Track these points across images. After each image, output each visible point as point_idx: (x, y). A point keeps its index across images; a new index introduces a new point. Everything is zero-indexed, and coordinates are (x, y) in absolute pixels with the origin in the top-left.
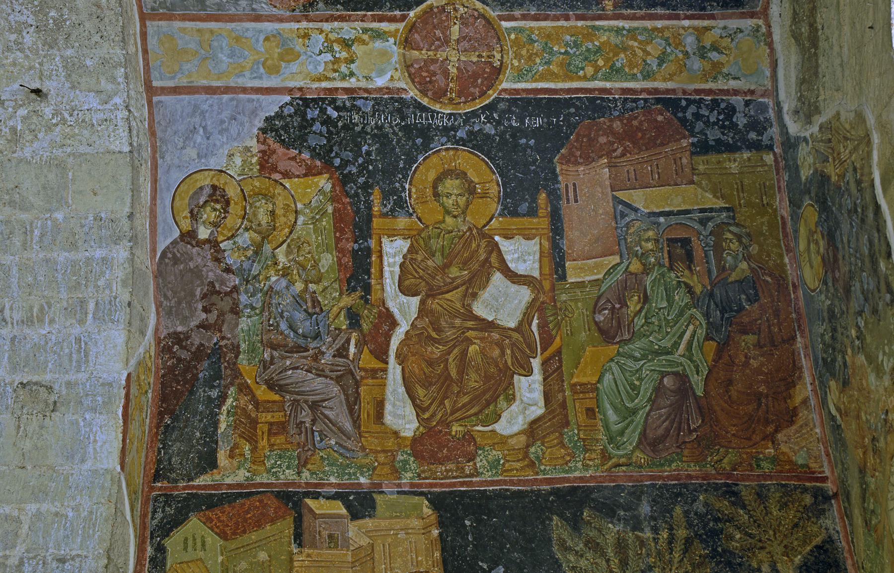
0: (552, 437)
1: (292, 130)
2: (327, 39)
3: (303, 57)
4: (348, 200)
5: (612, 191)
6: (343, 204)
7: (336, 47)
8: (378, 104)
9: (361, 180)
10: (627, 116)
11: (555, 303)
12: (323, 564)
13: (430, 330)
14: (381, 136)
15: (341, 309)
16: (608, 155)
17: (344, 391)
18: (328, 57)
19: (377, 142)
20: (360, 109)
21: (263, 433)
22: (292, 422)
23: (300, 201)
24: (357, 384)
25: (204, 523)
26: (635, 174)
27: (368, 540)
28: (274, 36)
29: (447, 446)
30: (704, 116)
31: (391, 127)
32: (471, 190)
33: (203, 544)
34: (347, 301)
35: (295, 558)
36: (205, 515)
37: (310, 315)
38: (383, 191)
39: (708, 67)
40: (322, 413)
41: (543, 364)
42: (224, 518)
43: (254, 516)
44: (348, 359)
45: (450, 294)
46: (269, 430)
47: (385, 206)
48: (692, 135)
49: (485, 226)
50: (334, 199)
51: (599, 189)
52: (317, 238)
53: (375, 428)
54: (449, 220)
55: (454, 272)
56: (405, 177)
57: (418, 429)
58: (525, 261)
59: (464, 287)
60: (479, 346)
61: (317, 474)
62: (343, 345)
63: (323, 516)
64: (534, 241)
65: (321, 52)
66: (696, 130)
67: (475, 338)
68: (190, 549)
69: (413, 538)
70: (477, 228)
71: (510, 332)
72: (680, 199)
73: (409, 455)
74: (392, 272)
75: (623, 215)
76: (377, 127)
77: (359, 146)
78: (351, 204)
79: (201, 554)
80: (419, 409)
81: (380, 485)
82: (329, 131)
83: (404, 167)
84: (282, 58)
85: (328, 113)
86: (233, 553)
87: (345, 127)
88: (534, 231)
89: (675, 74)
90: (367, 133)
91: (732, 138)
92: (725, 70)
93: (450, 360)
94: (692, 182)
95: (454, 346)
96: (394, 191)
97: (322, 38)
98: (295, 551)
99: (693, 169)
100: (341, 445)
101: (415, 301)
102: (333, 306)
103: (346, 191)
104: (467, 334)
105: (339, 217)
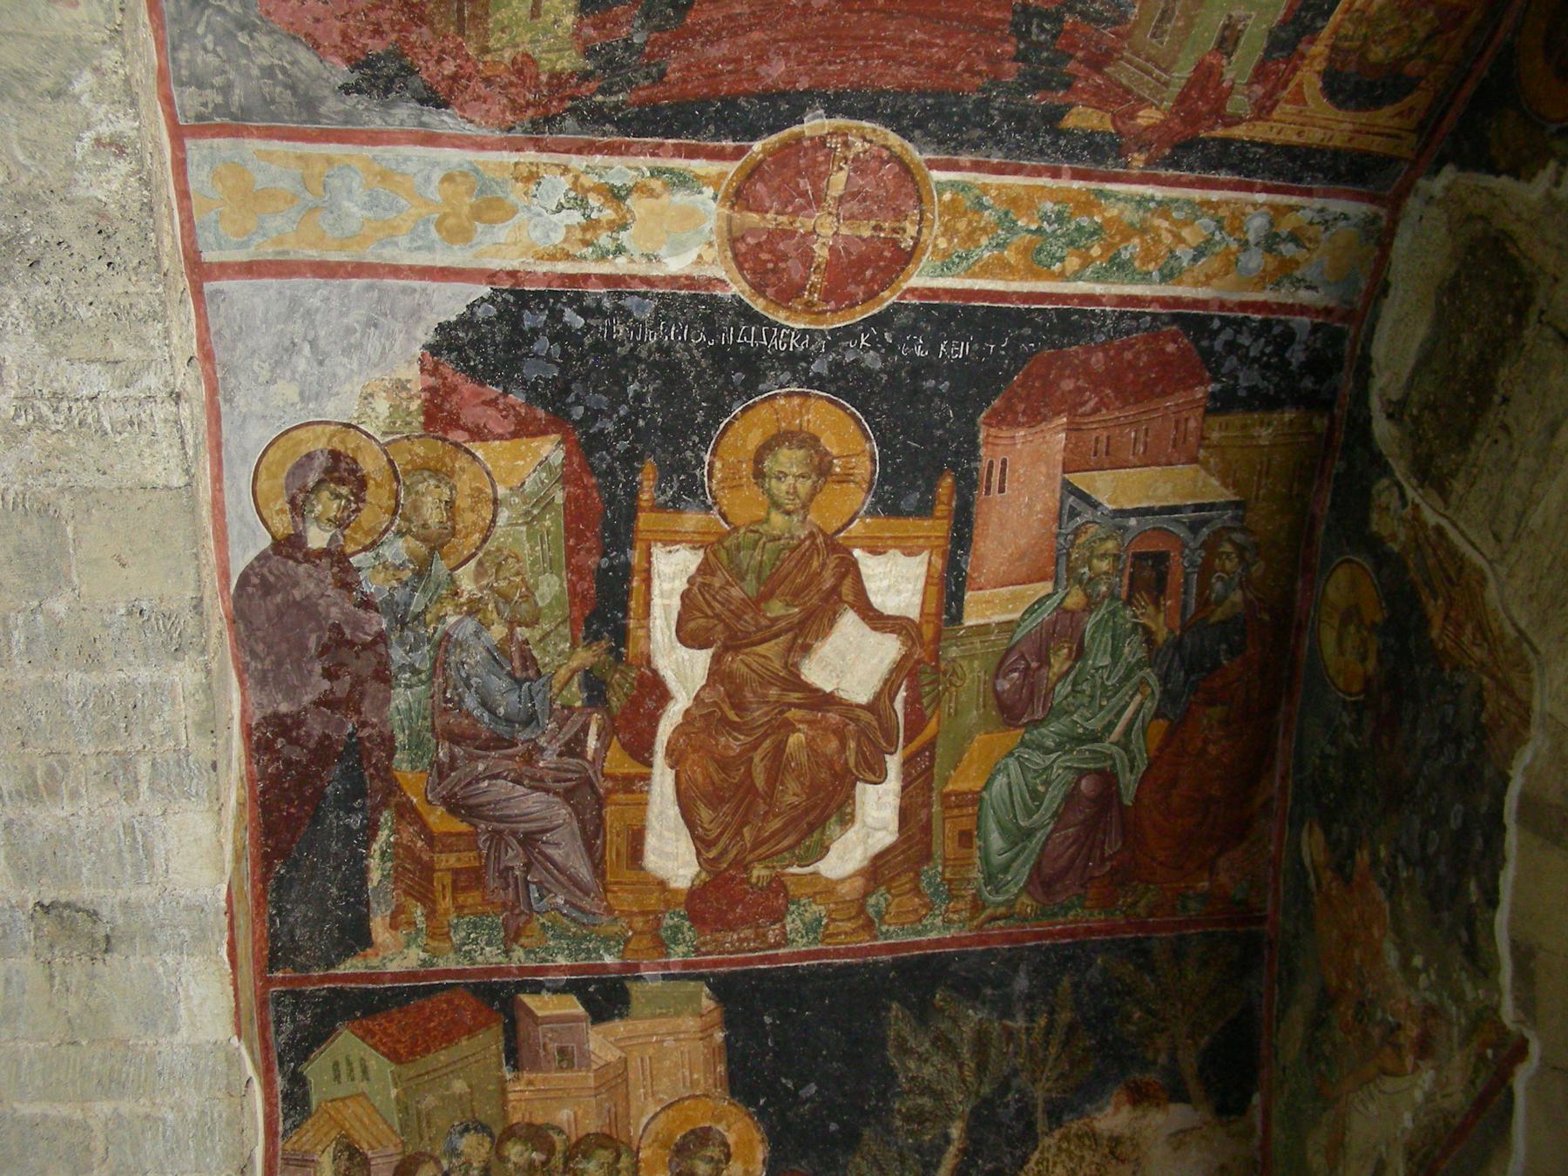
0: (904, 879)
1: (490, 350)
2: (575, 184)
3: (522, 216)
4: (594, 480)
5: (1064, 472)
6: (585, 487)
7: (594, 201)
8: (667, 306)
9: (622, 445)
10: (1117, 342)
11: (938, 661)
12: (552, 1094)
13: (726, 708)
14: (666, 367)
15: (574, 672)
16: (1072, 412)
17: (577, 814)
18: (576, 217)
19: (657, 377)
20: (630, 315)
21: (444, 887)
22: (498, 869)
23: (504, 482)
24: (600, 802)
25: (363, 1039)
26: (1108, 445)
27: (618, 1053)
28: (465, 175)
29: (742, 901)
30: (1241, 346)
31: (688, 350)
32: (822, 469)
33: (365, 1071)
34: (584, 657)
35: (510, 1087)
36: (361, 1025)
37: (520, 683)
38: (660, 465)
39: (1272, 263)
40: (541, 853)
41: (904, 764)
42: (393, 1030)
43: (440, 1024)
44: (585, 758)
45: (765, 646)
46: (454, 882)
47: (664, 492)
48: (1215, 379)
49: (839, 531)
50: (565, 480)
51: (1043, 469)
52: (532, 548)
53: (629, 875)
54: (777, 519)
55: (776, 608)
56: (705, 441)
57: (698, 875)
58: (899, 592)
59: (790, 635)
60: (806, 734)
61: (536, 953)
62: (576, 734)
63: (549, 1020)
64: (918, 558)
65: (560, 208)
66: (1223, 371)
67: (801, 722)
68: (344, 1077)
69: (686, 1046)
70: (825, 535)
71: (858, 711)
72: (1169, 486)
73: (683, 917)
74: (666, 608)
75: (1073, 514)
76: (660, 347)
77: (622, 384)
78: (598, 487)
79: (363, 1086)
80: (702, 842)
81: (636, 967)
82: (565, 354)
83: (705, 423)
84: (477, 214)
85: (566, 319)
86: (412, 1083)
87: (598, 346)
88: (921, 542)
89: (1215, 276)
90: (639, 360)
91: (1276, 386)
92: (1298, 274)
93: (757, 760)
94: (1194, 460)
95: (765, 736)
96: (683, 467)
97: (565, 183)
98: (509, 1076)
99: (1203, 438)
100: (573, 906)
101: (701, 660)
102: (560, 666)
103: (591, 465)
104: (789, 715)
105: (575, 515)
